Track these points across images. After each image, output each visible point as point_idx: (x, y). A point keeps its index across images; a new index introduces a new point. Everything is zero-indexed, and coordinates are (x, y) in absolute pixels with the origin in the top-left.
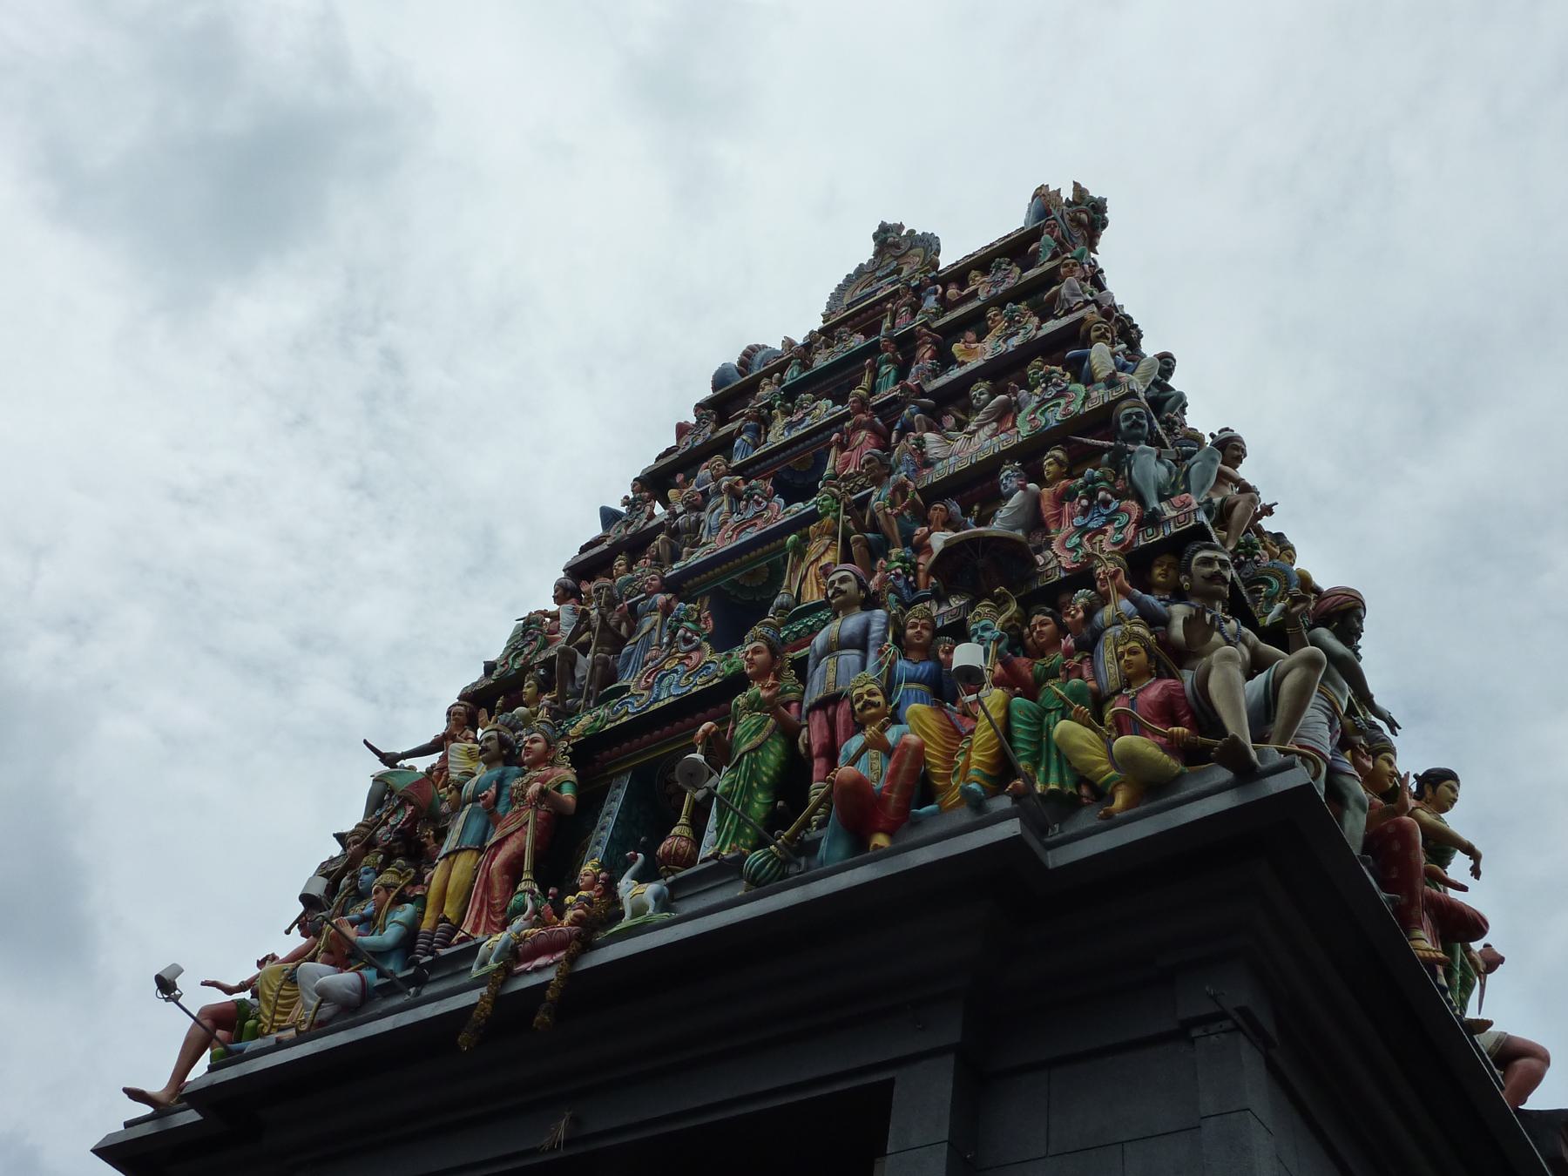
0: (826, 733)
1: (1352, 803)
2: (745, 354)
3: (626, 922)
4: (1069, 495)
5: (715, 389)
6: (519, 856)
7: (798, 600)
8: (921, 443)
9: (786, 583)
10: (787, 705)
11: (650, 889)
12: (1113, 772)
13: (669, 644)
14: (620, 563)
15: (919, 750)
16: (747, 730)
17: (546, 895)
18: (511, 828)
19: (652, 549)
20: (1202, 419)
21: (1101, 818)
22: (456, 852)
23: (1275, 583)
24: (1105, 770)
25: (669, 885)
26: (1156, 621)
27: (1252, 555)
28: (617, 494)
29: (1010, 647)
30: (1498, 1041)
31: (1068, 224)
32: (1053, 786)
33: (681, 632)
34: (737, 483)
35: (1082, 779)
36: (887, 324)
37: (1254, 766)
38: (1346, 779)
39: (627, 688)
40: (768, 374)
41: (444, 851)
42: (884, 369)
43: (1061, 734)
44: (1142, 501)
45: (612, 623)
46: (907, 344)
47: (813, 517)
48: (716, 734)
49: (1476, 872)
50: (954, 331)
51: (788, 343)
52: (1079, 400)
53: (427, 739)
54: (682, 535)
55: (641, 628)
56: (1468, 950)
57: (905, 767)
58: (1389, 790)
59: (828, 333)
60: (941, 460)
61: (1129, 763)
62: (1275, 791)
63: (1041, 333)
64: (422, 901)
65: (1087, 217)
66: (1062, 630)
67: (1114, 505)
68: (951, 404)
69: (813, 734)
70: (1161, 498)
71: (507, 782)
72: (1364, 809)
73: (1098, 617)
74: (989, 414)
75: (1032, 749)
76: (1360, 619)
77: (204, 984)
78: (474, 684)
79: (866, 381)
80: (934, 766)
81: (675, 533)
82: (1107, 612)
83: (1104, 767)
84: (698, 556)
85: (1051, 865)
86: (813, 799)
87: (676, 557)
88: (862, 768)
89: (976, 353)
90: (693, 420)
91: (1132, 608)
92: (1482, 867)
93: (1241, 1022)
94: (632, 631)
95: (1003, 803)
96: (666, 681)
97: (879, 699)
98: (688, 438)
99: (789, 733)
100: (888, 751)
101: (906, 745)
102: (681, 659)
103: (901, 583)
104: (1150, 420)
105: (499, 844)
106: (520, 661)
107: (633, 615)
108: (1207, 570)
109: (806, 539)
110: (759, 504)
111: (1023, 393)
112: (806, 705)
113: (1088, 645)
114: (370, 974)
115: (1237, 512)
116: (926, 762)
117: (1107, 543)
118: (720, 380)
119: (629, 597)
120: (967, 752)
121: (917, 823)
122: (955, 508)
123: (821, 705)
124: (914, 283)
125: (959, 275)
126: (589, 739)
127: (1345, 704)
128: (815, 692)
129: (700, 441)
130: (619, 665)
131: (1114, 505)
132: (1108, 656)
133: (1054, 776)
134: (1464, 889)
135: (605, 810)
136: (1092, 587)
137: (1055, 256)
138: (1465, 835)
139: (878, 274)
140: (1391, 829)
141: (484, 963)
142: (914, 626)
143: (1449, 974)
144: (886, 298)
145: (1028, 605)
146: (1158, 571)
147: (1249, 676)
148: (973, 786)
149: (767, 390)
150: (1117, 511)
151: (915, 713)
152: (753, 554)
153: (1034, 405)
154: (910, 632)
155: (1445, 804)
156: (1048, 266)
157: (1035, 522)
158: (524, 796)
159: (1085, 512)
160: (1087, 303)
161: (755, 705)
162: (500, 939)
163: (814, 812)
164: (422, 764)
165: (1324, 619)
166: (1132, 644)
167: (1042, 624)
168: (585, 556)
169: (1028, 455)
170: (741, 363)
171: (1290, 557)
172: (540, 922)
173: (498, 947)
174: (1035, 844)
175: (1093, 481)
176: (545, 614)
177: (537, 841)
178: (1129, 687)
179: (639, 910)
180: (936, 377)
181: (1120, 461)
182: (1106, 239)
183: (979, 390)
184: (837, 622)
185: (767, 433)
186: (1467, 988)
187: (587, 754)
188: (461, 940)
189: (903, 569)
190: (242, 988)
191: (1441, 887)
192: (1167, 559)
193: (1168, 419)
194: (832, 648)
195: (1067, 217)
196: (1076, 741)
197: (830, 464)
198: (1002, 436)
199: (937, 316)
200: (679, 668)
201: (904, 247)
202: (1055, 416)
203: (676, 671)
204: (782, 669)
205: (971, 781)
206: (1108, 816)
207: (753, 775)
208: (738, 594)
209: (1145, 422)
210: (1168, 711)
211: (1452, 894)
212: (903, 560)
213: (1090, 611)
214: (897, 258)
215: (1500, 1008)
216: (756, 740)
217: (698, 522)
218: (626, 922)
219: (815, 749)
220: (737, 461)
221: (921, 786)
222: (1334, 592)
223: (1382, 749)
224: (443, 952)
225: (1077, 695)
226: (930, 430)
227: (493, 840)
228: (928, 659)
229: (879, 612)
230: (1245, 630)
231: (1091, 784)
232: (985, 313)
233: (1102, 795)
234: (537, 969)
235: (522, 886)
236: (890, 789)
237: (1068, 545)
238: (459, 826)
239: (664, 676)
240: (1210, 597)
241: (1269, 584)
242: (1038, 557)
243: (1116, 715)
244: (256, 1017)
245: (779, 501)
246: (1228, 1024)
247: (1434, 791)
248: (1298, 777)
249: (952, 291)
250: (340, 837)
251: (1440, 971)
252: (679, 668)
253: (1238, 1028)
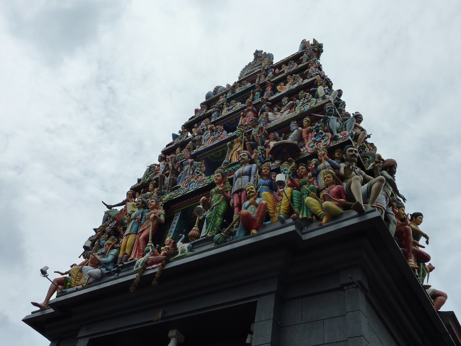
0: (238, 200)
1: (392, 222)
2: (215, 88)
3: (179, 255)
4: (311, 131)
5: (206, 99)
6: (148, 236)
7: (230, 161)
8: (267, 115)
9: (227, 156)
10: (227, 192)
11: (186, 245)
12: (322, 212)
13: (192, 174)
14: (178, 150)
15: (266, 205)
16: (215, 199)
17: (156, 247)
18: (146, 227)
19: (187, 146)
20: (350, 109)
21: (319, 225)
22: (129, 234)
23: (371, 157)
24: (320, 212)
25: (192, 244)
26: (336, 168)
27: (364, 149)
28: (177, 130)
29: (293, 176)
30: (433, 291)
31: (312, 50)
32: (305, 216)
33: (196, 170)
34: (213, 127)
35: (313, 214)
36: (257, 80)
37: (364, 211)
38: (390, 215)
39: (180, 187)
40: (222, 95)
41: (126, 234)
42: (256, 93)
43: (307, 201)
44: (332, 133)
45: (176, 168)
46: (263, 86)
47: (235, 137)
48: (206, 200)
49: (427, 243)
50: (277, 82)
51: (228, 86)
52: (314, 103)
53: (121, 201)
54: (196, 142)
55: (184, 169)
56: (424, 265)
57: (261, 210)
58: (403, 219)
59: (240, 83)
60: (273, 120)
61: (327, 209)
62: (370, 218)
63: (303, 83)
64: (119, 248)
65: (317, 49)
66: (308, 171)
67: (324, 134)
68: (276, 104)
69: (235, 201)
70: (338, 132)
71: (144, 214)
72: (395, 224)
73: (319, 167)
74: (287, 107)
75: (299, 205)
76: (395, 168)
77: (55, 272)
78: (135, 185)
79: (251, 97)
80: (270, 210)
81: (194, 141)
82: (321, 166)
83: (320, 211)
84: (201, 148)
85: (304, 239)
86: (234, 220)
87: (194, 148)
88: (249, 210)
89: (283, 89)
90: (200, 108)
91: (329, 164)
92: (429, 241)
93: (358, 285)
94: (181, 170)
95: (290, 221)
96: (191, 185)
97: (254, 190)
98: (198, 113)
99: (227, 200)
100: (257, 205)
101: (262, 204)
103: (261, 156)
104: (335, 109)
105: (142, 232)
106: (148, 178)
107: (182, 165)
108: (351, 153)
109: (233, 143)
110: (219, 133)
111: (298, 101)
112: (232, 192)
113: (316, 175)
114: (104, 270)
115: (360, 137)
116: (268, 209)
117: (321, 145)
118: (208, 96)
119: (180, 160)
120: (280, 206)
121: (265, 226)
122: (277, 135)
123: (237, 192)
124: (266, 68)
125: (279, 66)
126: (168, 201)
127: (390, 193)
128: (235, 188)
129: (202, 114)
130: (177, 180)
131: (324, 134)
132: (321, 178)
133: (305, 213)
134: (424, 247)
135: (173, 222)
136: (317, 158)
137: (307, 60)
138: (425, 232)
139: (255, 65)
140: (403, 230)
141: (137, 267)
142: (265, 169)
143: (419, 272)
144: (257, 73)
145: (298, 163)
146: (336, 153)
147: (363, 185)
148: (281, 216)
149: (222, 100)
150: (325, 136)
151: (265, 194)
152: (217, 148)
153: (301, 104)
154: (263, 171)
155: (419, 223)
156: (305, 63)
157: (301, 139)
158: (149, 218)
159: (315, 136)
160: (317, 74)
161: (218, 192)
162: (142, 259)
163: (234, 223)
164: (119, 208)
165: (385, 168)
166: (329, 175)
167: (302, 169)
168: (168, 148)
169: (299, 119)
170: (214, 91)
171: (375, 150)
172: (154, 254)
173: (141, 262)
174: (299, 232)
175: (318, 127)
176: (156, 165)
177: (153, 231)
178: (327, 187)
179: (183, 251)
180: (272, 96)
181: (326, 121)
182: (322, 56)
183: (285, 100)
184: (242, 168)
185: (222, 112)
186: (424, 276)
187: (168, 206)
188: (131, 260)
189: (262, 152)
190: (66, 273)
191: (417, 247)
192: (339, 150)
193: (340, 109)
194: (240, 175)
195: (311, 49)
196: (311, 203)
197: (240, 122)
198: (291, 114)
199: (272, 78)
200: (195, 181)
201: (263, 58)
202: (307, 108)
203: (194, 182)
204: (225, 181)
205: (281, 214)
206: (321, 225)
207: (217, 212)
208: (213, 159)
209: (333, 110)
210: (339, 194)
211: (420, 249)
212: (262, 150)
213: (316, 165)
214: (261, 61)
215: (433, 282)
216: (218, 202)
217: (201, 138)
218: (179, 255)
219: (235, 205)
220: (213, 120)
221: (266, 216)
222: (388, 160)
223: (401, 206)
224: (125, 263)
225: (312, 190)
226: (270, 111)
227: (140, 231)
228: (269, 179)
229: (255, 165)
230: (362, 171)
231: (316, 216)
232: (287, 77)
233: (319, 219)
234: (153, 268)
235: (149, 244)
236: (257, 216)
237: (310, 146)
238: (130, 227)
239: (191, 183)
240: (352, 161)
241: (369, 158)
242: (301, 149)
243: (324, 196)
244: (70, 282)
245: (225, 132)
246: (355, 285)
248: (377, 214)
249: (277, 71)
250: (95, 230)
251: (416, 271)
252: (195, 181)
253: (357, 287)
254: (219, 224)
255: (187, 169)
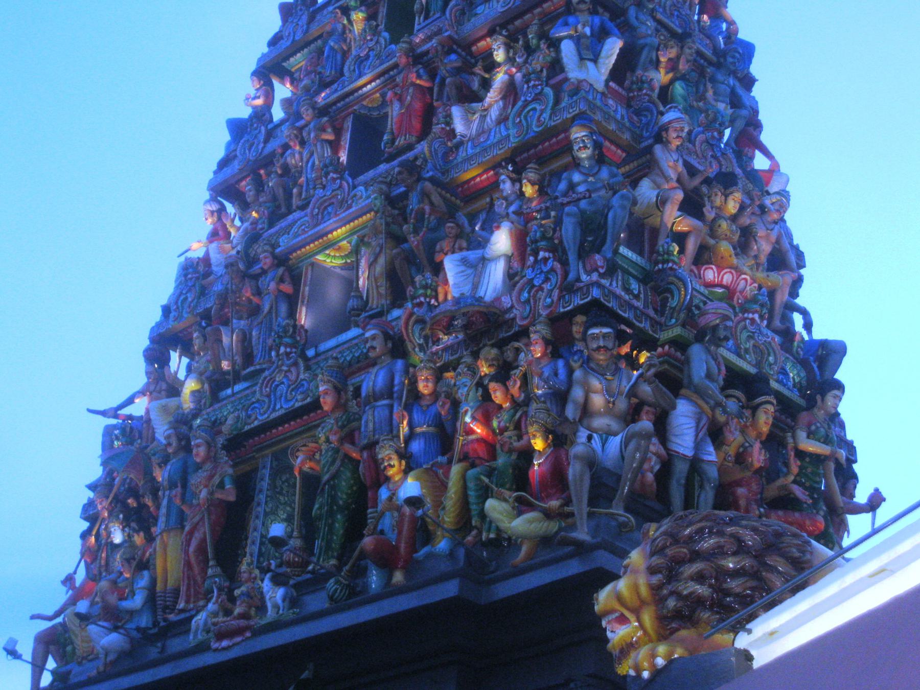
6: (204, 540)
18: (197, 518)
33: (282, 350)
77: (33, 617)
102: (286, 372)
173: (201, 623)
203: (283, 383)
204: (347, 400)
207: (333, 499)
216: (333, 469)
234: (224, 649)
235: (210, 571)
239: (277, 386)
244: (72, 643)
247: (823, 400)
254: (341, 532)
255: (271, 308)
